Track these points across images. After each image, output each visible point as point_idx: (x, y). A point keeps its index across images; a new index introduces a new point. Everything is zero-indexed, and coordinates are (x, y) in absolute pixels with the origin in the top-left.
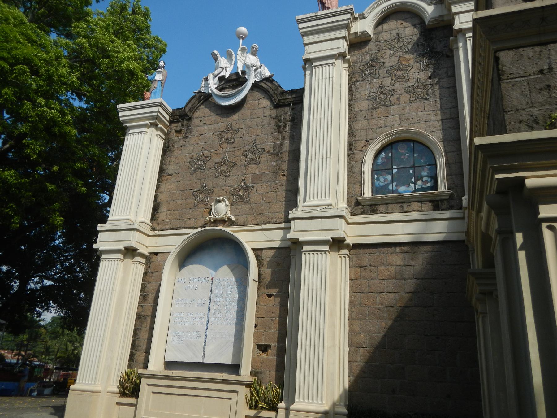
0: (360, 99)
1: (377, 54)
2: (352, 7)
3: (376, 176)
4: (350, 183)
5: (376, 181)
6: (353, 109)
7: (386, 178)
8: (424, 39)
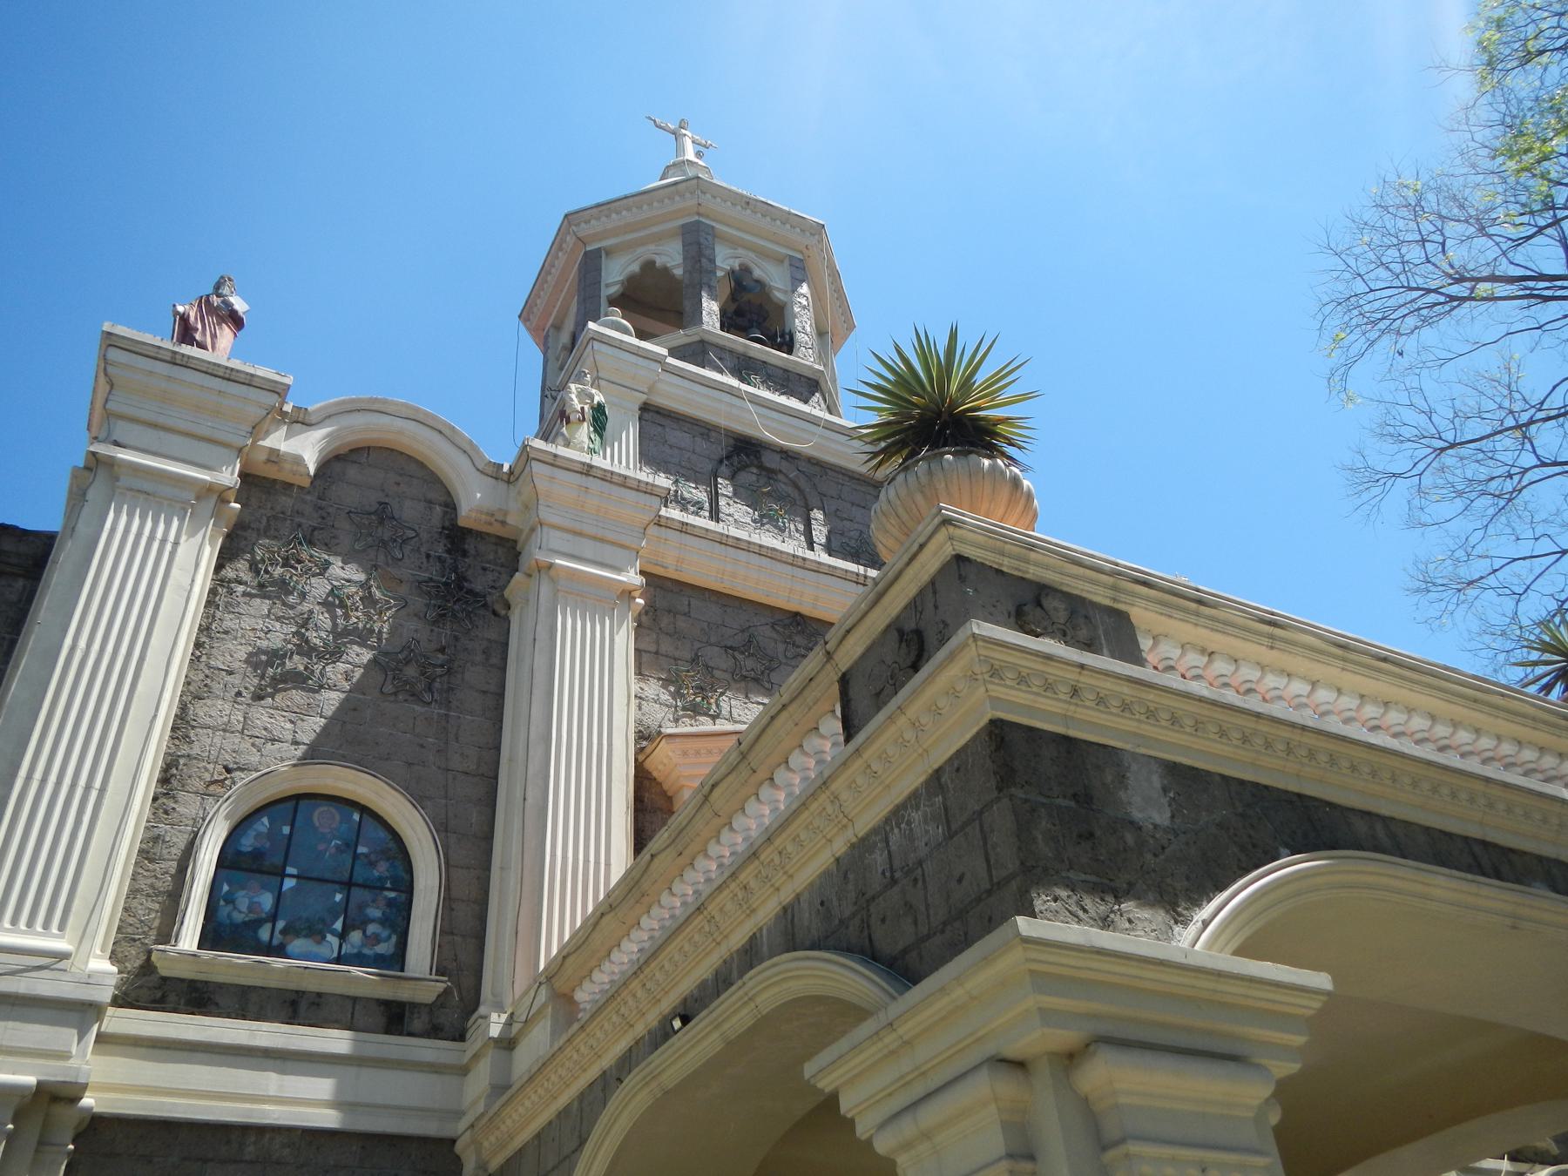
0: (236, 638)
1: (316, 533)
2: (289, 380)
3: (226, 888)
4: (137, 891)
5: (222, 903)
6: (204, 658)
7: (256, 899)
8: (445, 546)
